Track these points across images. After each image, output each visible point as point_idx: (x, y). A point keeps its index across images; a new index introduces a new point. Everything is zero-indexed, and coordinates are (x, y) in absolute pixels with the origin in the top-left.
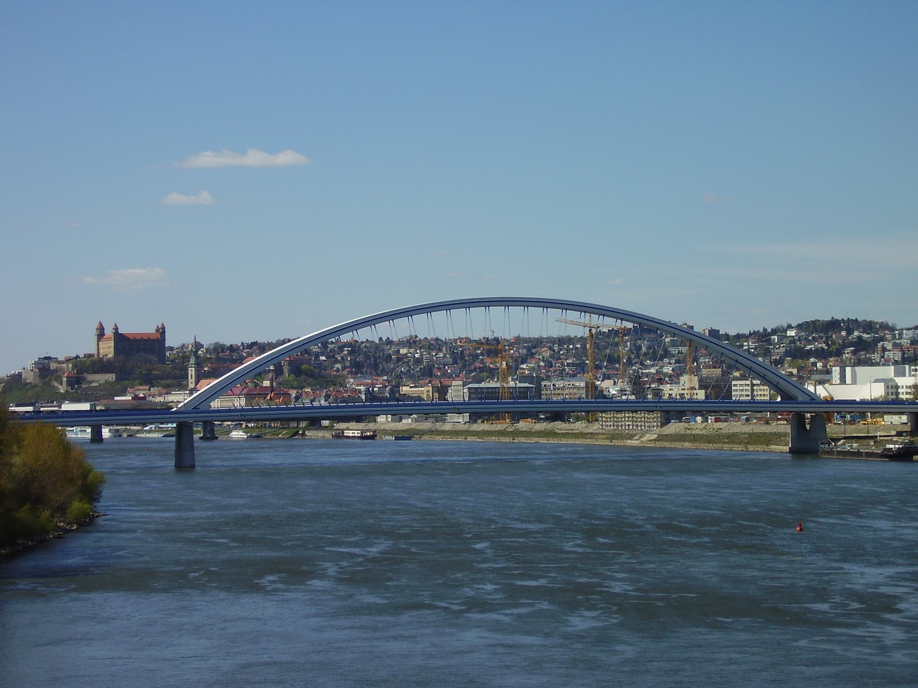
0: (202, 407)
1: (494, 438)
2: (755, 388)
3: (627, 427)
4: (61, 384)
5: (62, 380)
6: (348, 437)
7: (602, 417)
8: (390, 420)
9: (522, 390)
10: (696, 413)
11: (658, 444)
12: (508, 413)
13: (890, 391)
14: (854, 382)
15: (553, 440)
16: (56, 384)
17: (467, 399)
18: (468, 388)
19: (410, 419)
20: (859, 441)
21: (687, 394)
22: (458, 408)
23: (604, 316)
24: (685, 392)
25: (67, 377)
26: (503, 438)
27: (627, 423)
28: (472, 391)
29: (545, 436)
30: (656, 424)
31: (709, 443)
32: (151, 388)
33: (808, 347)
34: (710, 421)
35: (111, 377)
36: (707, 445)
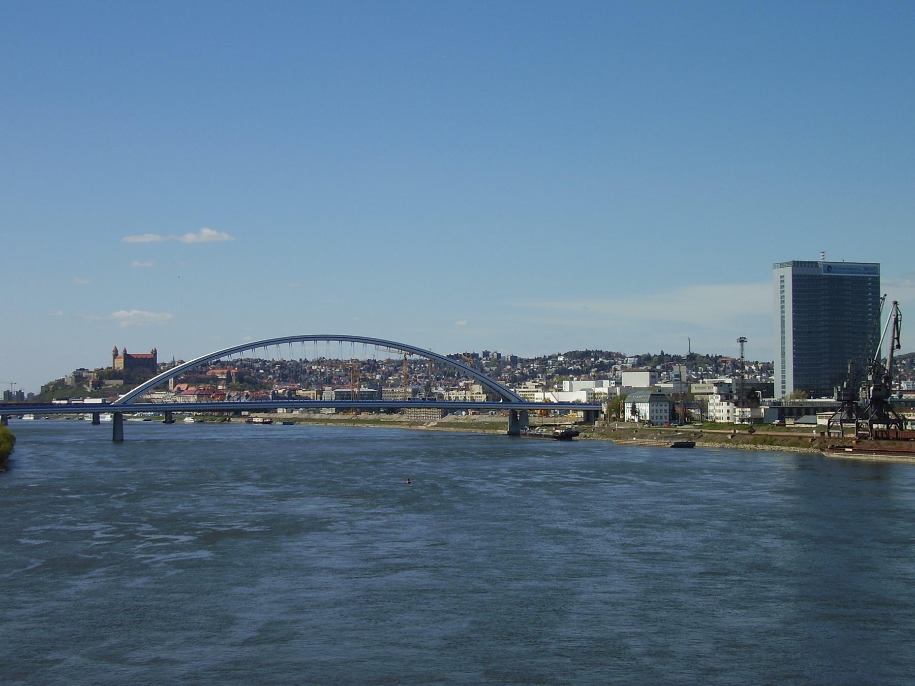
4: (89, 386)
6: (255, 423)
7: (408, 411)
8: (285, 411)
9: (369, 393)
10: (463, 409)
11: (436, 429)
12: (359, 408)
13: (590, 396)
14: (571, 390)
16: (85, 386)
17: (333, 399)
20: (547, 427)
22: (328, 404)
24: (473, 395)
27: (422, 415)
28: (338, 393)
29: (372, 423)
30: (438, 416)
33: (570, 368)
34: (469, 414)
35: (121, 382)
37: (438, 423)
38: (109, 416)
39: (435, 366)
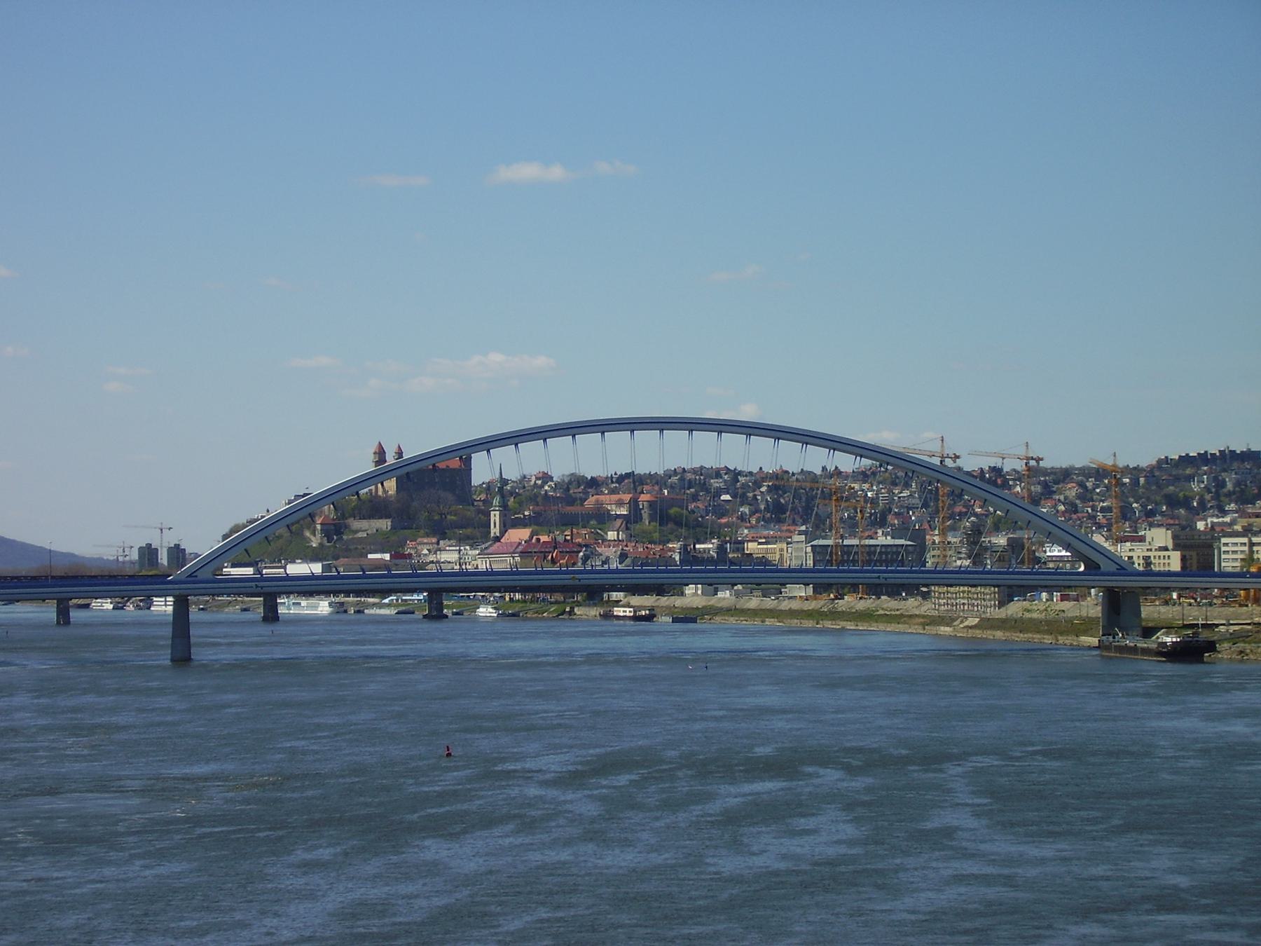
1: (796, 621)
2: (1255, 548)
3: (962, 606)
5: (315, 527)
6: (618, 617)
8: (699, 592)
15: (862, 626)
16: (307, 534)
17: (810, 563)
18: (812, 546)
19: (728, 592)
21: (1155, 557)
24: (1151, 554)
25: (321, 524)
26: (807, 621)
27: (962, 601)
28: (818, 549)
29: (855, 620)
31: (1021, 632)
32: (441, 541)
34: (1055, 600)
35: (385, 524)
37: (982, 619)
38: (326, 603)
39: (1147, 482)
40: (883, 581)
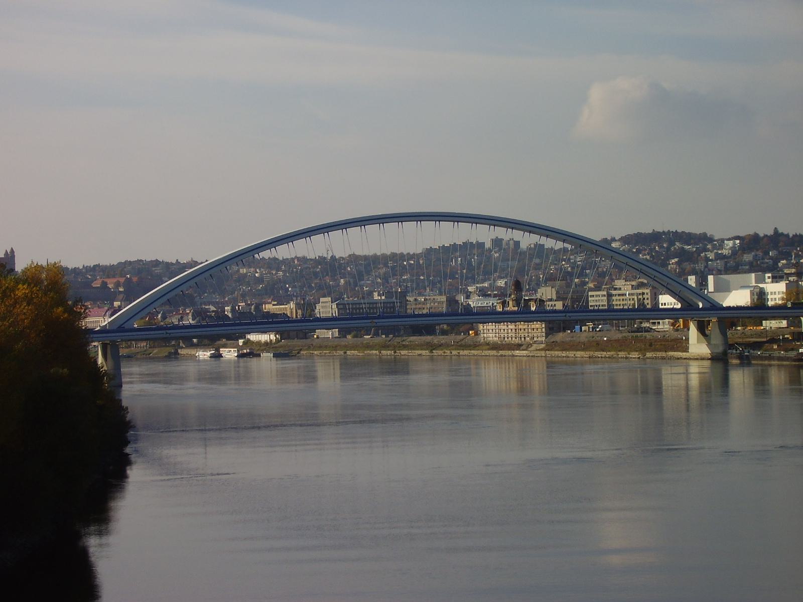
0: (127, 326)
22: (327, 322)
23: (512, 229)
31: (603, 351)
36: (602, 353)
40: (568, 318)
